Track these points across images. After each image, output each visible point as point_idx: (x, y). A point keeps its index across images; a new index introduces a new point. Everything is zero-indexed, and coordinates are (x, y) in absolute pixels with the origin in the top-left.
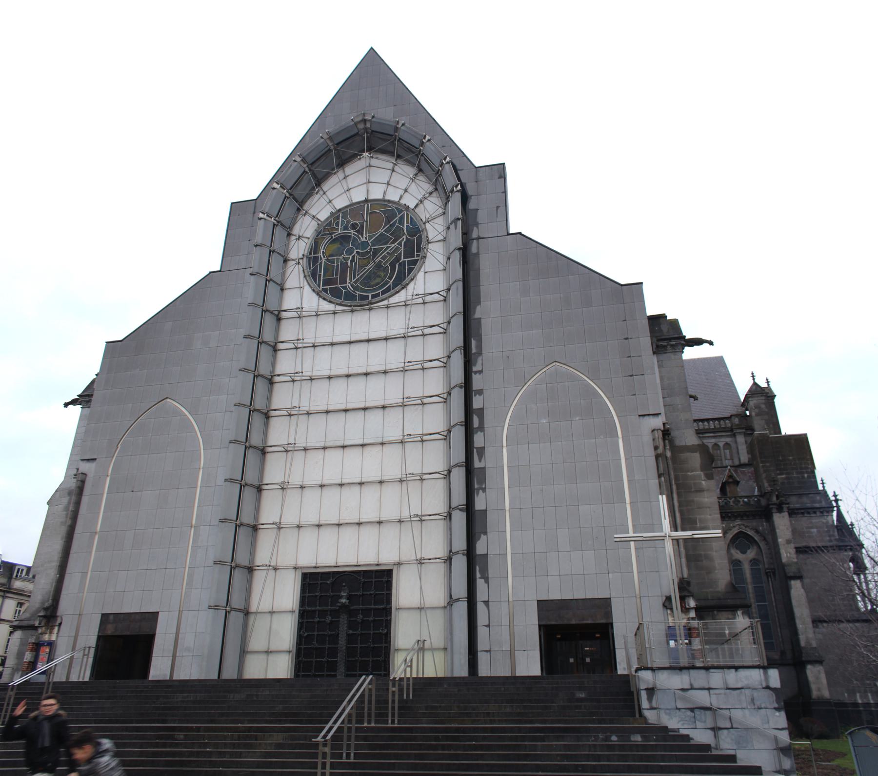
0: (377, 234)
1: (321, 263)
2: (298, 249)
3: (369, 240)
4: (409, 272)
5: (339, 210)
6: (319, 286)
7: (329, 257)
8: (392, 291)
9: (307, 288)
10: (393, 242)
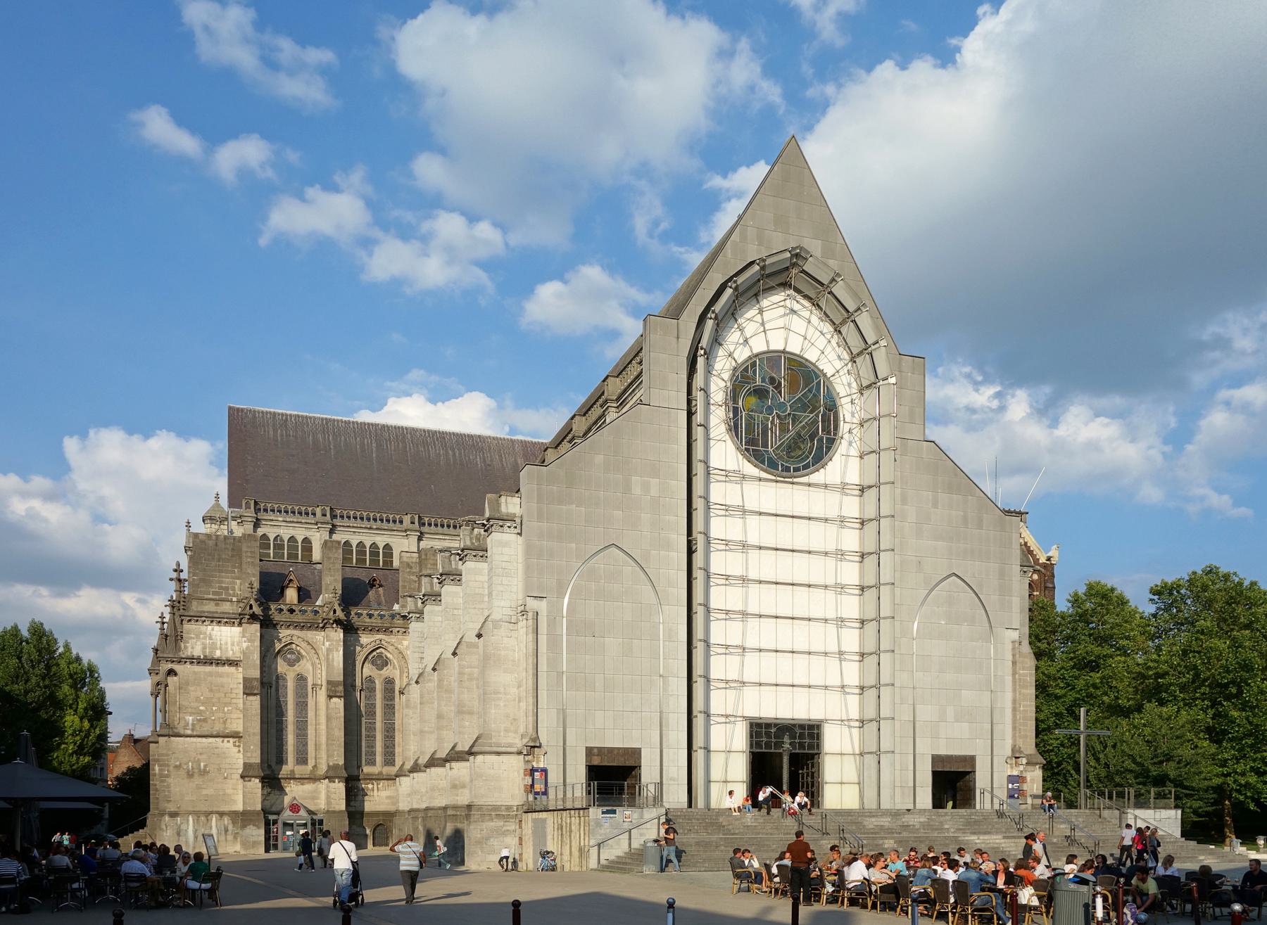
0: (795, 397)
1: (741, 416)
4: (829, 449)
5: (757, 355)
9: (729, 442)
10: (811, 412)
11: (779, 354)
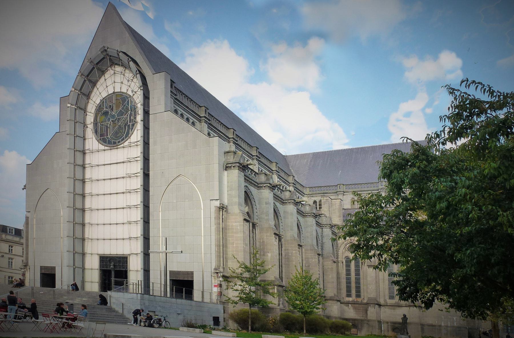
2: (90, 119)
3: (116, 114)
5: (104, 98)
6: (98, 137)
7: (101, 123)
8: (125, 140)
9: (94, 138)
10: (125, 115)
11: (113, 94)
